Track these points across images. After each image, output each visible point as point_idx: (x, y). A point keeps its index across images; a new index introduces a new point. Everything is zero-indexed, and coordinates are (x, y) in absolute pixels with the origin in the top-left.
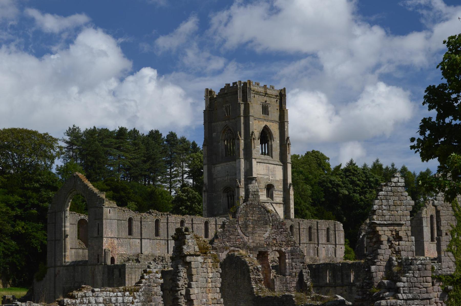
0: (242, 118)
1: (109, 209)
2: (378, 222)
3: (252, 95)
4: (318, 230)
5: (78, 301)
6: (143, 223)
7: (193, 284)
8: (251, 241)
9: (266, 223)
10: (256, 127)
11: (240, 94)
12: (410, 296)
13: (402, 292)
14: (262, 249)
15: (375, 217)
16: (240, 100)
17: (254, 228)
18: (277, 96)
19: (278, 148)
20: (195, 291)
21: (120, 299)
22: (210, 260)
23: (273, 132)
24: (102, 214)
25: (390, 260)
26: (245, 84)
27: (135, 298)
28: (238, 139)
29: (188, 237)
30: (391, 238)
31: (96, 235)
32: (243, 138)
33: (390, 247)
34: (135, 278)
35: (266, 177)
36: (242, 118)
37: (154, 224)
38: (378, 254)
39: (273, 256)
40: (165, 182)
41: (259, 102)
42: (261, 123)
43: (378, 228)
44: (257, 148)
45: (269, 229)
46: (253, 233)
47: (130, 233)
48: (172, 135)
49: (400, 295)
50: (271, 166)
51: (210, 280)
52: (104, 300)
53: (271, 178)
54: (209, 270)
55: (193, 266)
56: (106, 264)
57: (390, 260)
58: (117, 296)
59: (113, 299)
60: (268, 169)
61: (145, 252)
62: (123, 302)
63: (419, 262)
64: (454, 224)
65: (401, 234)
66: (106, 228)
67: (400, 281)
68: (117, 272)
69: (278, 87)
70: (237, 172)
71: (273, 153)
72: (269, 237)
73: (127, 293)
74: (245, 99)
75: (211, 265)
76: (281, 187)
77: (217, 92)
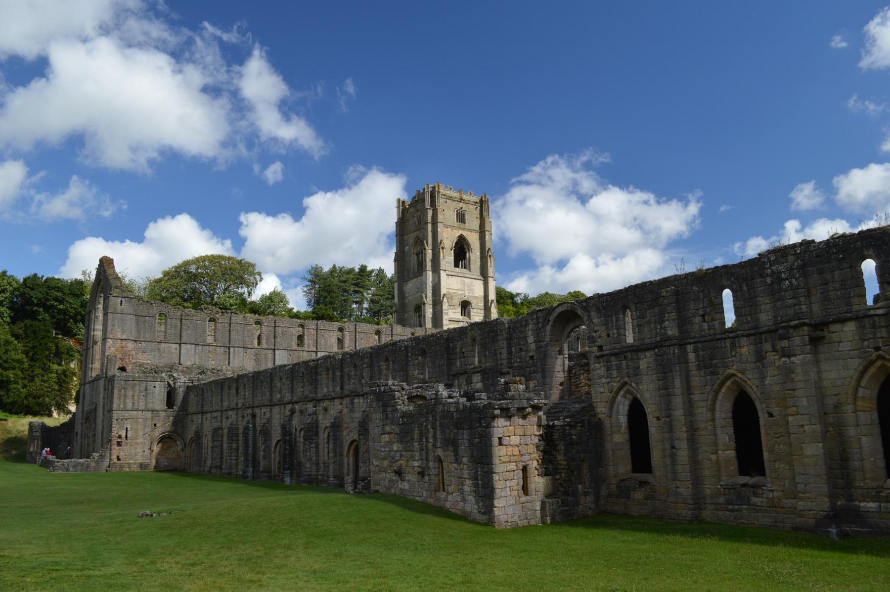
0: (430, 226)
1: (120, 299)
3: (442, 200)
6: (184, 322)
10: (448, 237)
16: (428, 205)
18: (476, 203)
19: (479, 260)
23: (471, 242)
32: (430, 247)
34: (133, 396)
35: (460, 292)
41: (453, 209)
42: (455, 231)
53: (467, 294)
66: (114, 325)
76: (482, 304)
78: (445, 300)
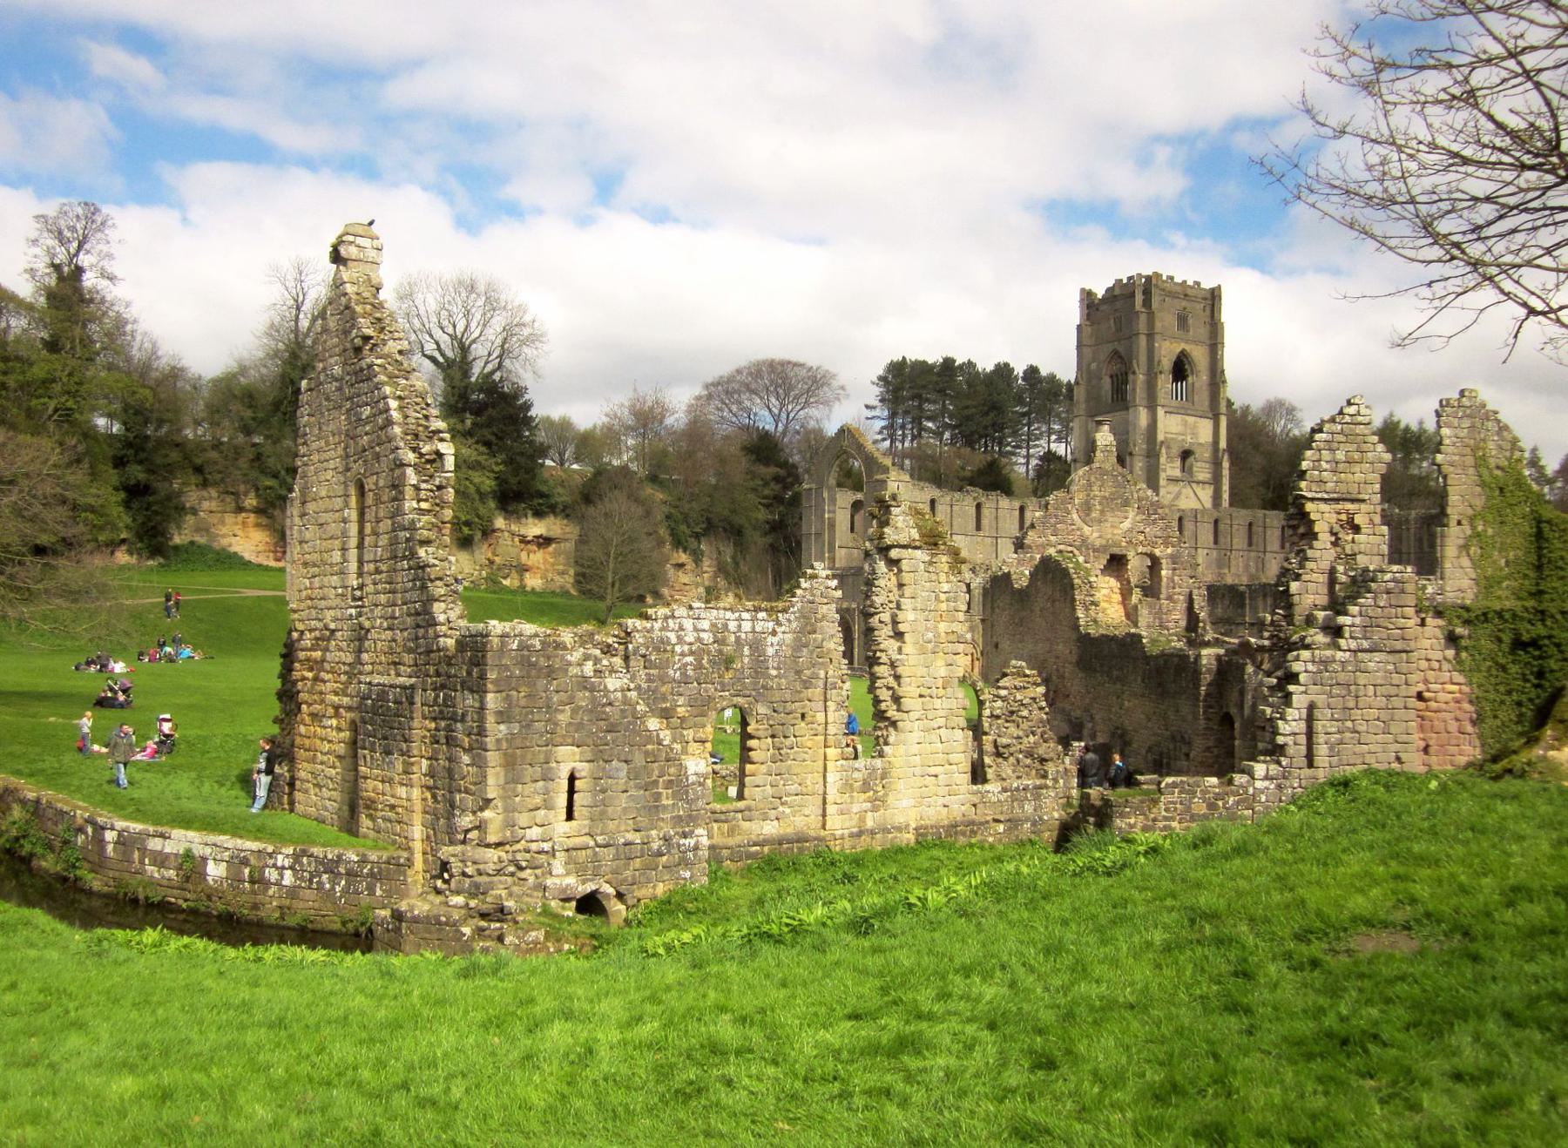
2: (1309, 495)
5: (657, 625)
7: (906, 603)
8: (1096, 535)
9: (1126, 503)
10: (1167, 351)
11: (1139, 298)
12: (1366, 644)
13: (1347, 635)
14: (1116, 551)
15: (1303, 484)
17: (1102, 512)
20: (908, 617)
21: (747, 626)
22: (944, 559)
25: (1332, 572)
26: (1149, 278)
27: (779, 623)
29: (894, 511)
30: (1337, 528)
33: (1335, 544)
38: (1307, 559)
39: (1136, 566)
40: (1019, 447)
43: (1309, 507)
44: (1165, 383)
45: (1131, 514)
46: (1100, 522)
48: (1032, 372)
49: (1342, 642)
50: (1191, 419)
51: (943, 597)
52: (713, 625)
54: (943, 577)
55: (905, 565)
57: (1332, 572)
58: (740, 619)
59: (732, 626)
60: (1185, 424)
62: (754, 631)
63: (1388, 576)
64: (1479, 503)
65: (1358, 520)
67: (1346, 613)
72: (1130, 530)
73: (762, 615)
74: (1147, 303)
75: (946, 568)
77: (1100, 293)
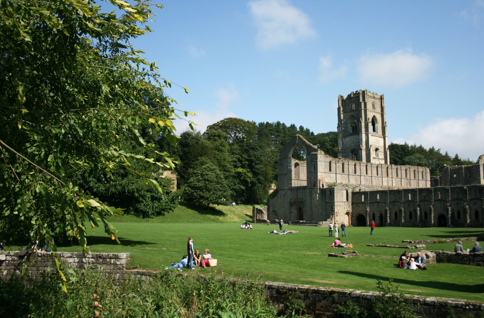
4: (418, 172)
10: (370, 116)
16: (361, 100)
24: (316, 158)
26: (364, 92)
28: (361, 122)
31: (312, 170)
35: (375, 144)
36: (363, 111)
37: (341, 166)
47: (330, 170)
56: (320, 188)
61: (339, 182)
68: (328, 193)
69: (380, 94)
70: (360, 141)
71: (378, 131)
77: (345, 97)
78: (371, 148)
